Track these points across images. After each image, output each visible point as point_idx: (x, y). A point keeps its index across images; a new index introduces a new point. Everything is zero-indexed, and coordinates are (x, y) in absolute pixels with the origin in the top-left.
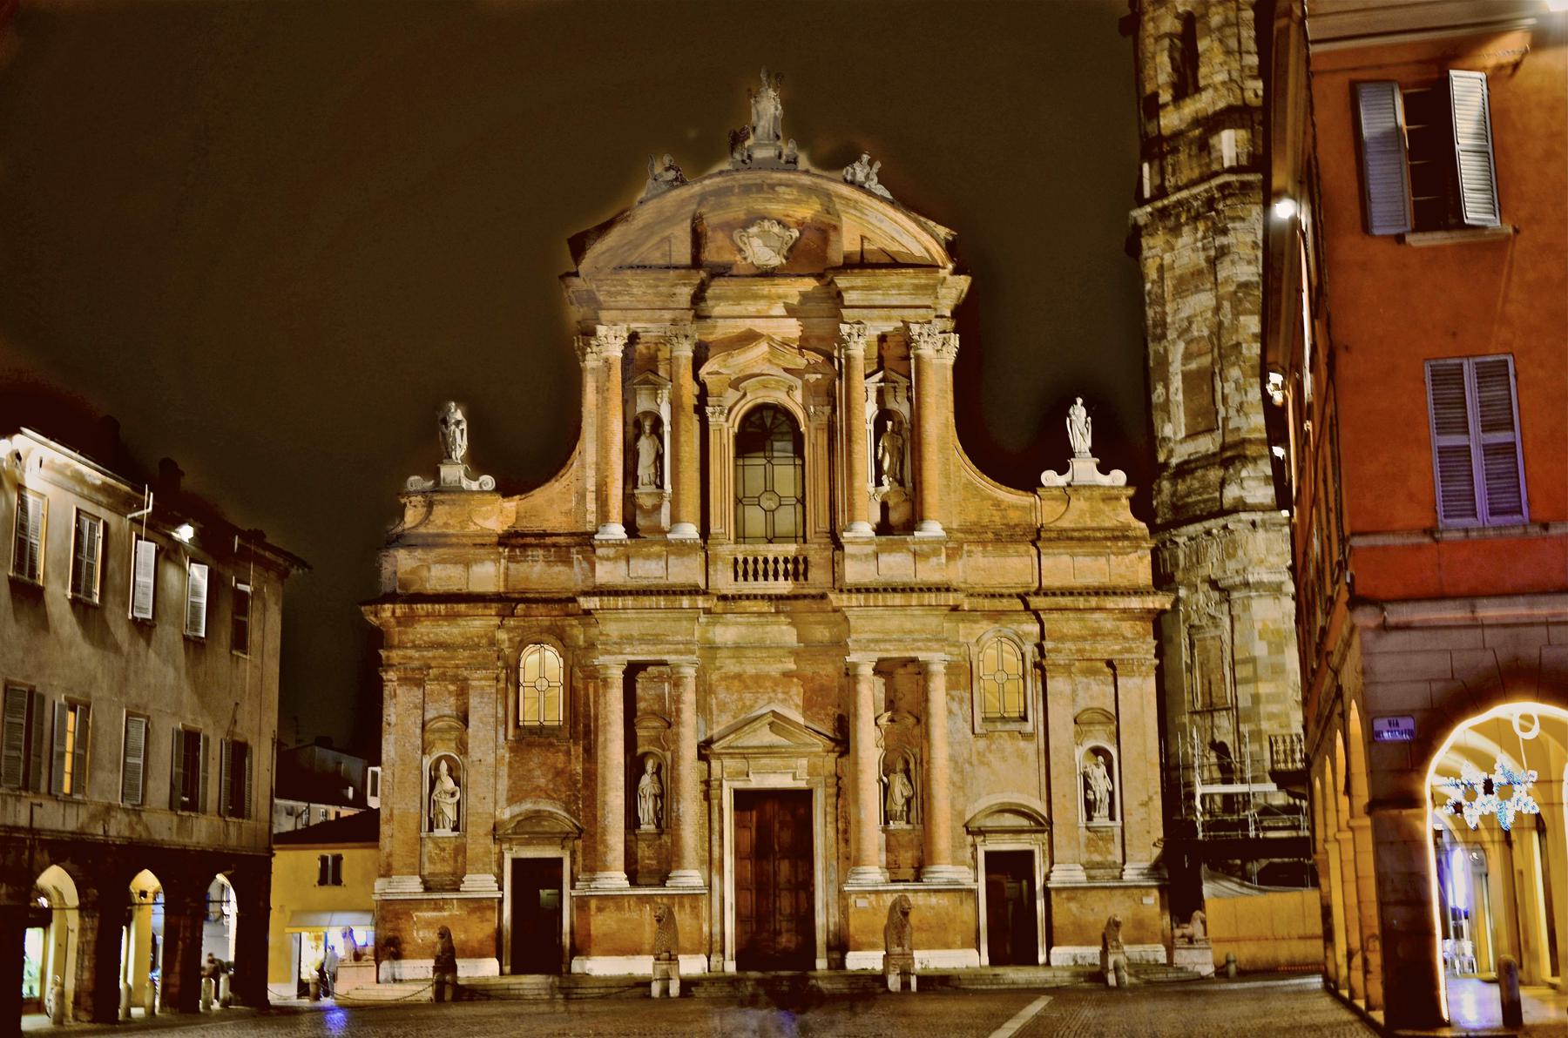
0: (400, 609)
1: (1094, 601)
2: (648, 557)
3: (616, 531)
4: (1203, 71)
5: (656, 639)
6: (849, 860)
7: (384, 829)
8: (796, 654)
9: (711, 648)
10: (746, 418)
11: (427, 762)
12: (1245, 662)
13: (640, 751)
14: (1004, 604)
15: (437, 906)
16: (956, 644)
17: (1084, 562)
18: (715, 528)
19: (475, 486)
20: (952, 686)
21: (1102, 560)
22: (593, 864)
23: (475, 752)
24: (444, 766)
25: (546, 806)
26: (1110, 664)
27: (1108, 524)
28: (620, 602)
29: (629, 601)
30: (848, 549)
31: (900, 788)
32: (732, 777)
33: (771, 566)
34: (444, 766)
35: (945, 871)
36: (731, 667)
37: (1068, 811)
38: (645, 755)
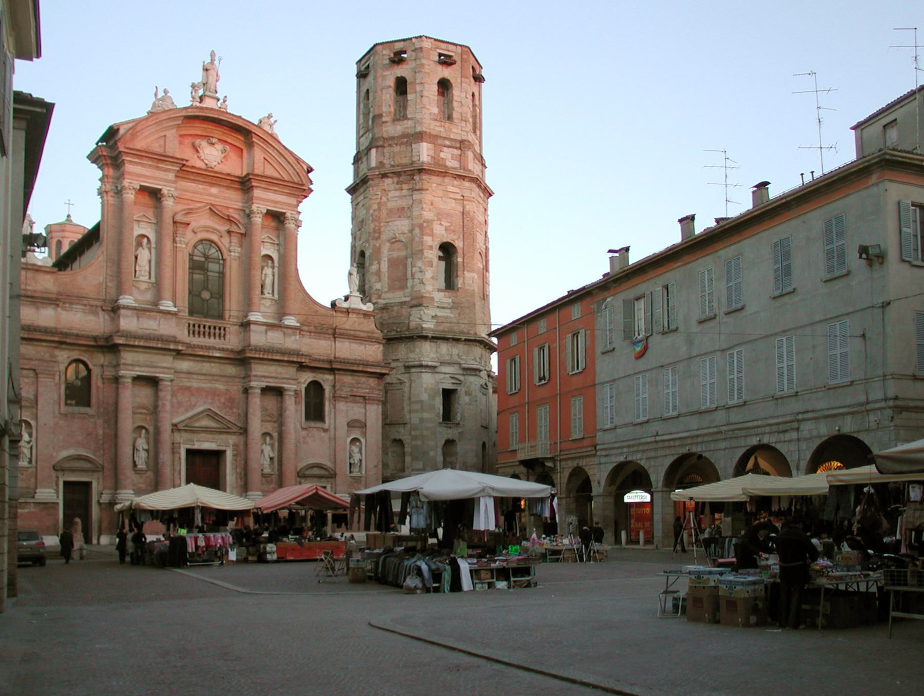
2: (149, 318)
10: (195, 247)
12: (417, 402)
21: (363, 347)
23: (42, 421)
25: (84, 453)
27: (365, 329)
37: (343, 469)
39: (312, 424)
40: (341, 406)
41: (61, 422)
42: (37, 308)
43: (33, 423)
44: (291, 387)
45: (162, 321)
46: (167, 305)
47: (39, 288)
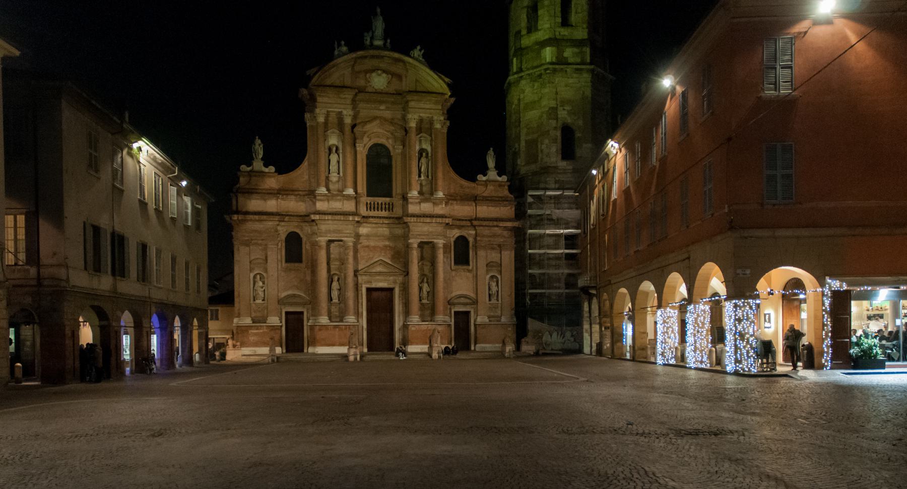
1: (495, 223)
2: (337, 200)
3: (323, 190)
4: (540, 22)
5: (339, 232)
6: (407, 312)
7: (236, 300)
8: (389, 239)
9: (358, 236)
11: (252, 275)
14: (464, 223)
17: (492, 209)
18: (360, 190)
19: (266, 170)
20: (444, 253)
21: (498, 209)
22: (315, 313)
24: (258, 277)
26: (499, 246)
28: (326, 217)
29: (330, 217)
30: (410, 200)
31: (426, 287)
32: (365, 283)
34: (258, 277)
35: (440, 318)
37: (484, 298)
39: (460, 267)
41: (283, 274)
44: (440, 242)
45: (345, 202)
47: (266, 187)
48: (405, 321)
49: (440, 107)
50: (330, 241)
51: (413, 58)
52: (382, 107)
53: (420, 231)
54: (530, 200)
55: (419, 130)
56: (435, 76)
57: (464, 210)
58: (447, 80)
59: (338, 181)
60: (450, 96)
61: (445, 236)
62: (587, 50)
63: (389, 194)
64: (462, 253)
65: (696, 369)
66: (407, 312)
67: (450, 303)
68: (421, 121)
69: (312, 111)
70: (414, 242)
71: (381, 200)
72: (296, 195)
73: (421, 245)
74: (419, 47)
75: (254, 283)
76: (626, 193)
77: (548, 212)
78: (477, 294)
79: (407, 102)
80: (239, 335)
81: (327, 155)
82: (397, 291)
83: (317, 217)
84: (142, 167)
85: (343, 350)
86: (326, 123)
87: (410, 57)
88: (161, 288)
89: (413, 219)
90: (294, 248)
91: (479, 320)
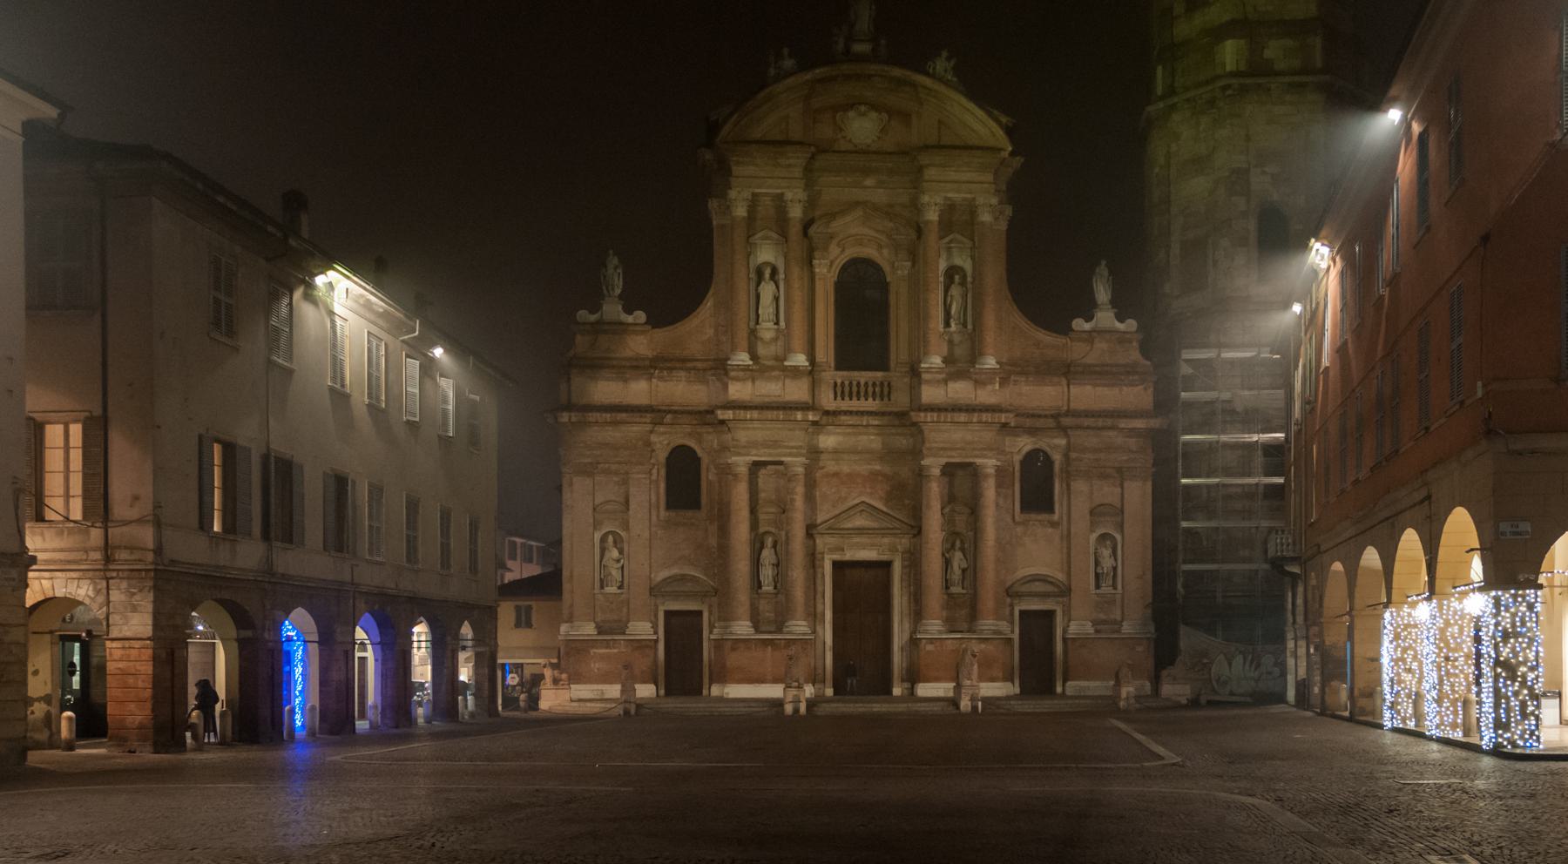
0: (575, 417)
1: (1109, 422)
3: (742, 358)
5: (775, 444)
6: (917, 613)
7: (566, 586)
9: (814, 453)
10: (844, 268)
11: (598, 536)
13: (762, 530)
14: (1040, 423)
15: (607, 644)
16: (1002, 452)
19: (630, 319)
20: (999, 486)
21: (1116, 390)
22: (726, 616)
24: (610, 538)
29: (755, 414)
30: (924, 376)
31: (958, 560)
32: (832, 551)
33: (862, 389)
34: (610, 538)
35: (987, 624)
36: (830, 466)
37: (1084, 581)
38: (767, 533)
39: (1033, 516)
40: (1080, 486)
42: (626, 381)
43: (623, 534)
44: (989, 464)
46: (800, 360)
47: (628, 353)
48: (914, 632)
49: (989, 177)
50: (757, 466)
51: (932, 76)
52: (869, 182)
53: (947, 441)
54: (1186, 370)
55: (947, 226)
56: (980, 113)
57: (1044, 395)
58: (1004, 120)
59: (776, 339)
60: (1012, 154)
61: (1001, 451)
62: (1317, 42)
63: (883, 366)
64: (1037, 488)
65: (1440, 740)
66: (917, 613)
67: (1011, 593)
68: (950, 208)
69: (723, 196)
70: (933, 465)
71: (864, 377)
72: (688, 370)
73: (949, 470)
74: (945, 54)
75: (603, 551)
76: (1341, 351)
77: (1226, 395)
78: (1069, 575)
79: (921, 169)
80: (571, 659)
81: (753, 285)
82: (897, 568)
83: (729, 415)
84: (339, 322)
85: (774, 691)
86: (751, 218)
87: (927, 74)
88: (380, 564)
89: (929, 416)
90: (684, 482)
91: (1074, 628)
